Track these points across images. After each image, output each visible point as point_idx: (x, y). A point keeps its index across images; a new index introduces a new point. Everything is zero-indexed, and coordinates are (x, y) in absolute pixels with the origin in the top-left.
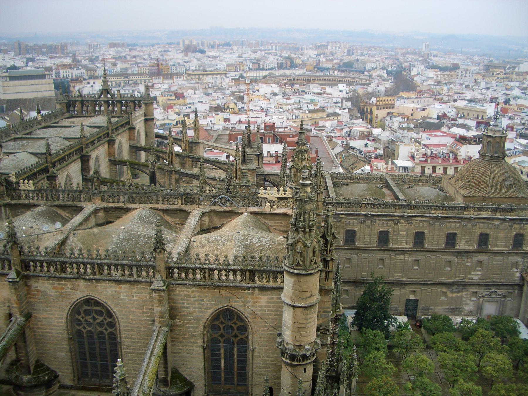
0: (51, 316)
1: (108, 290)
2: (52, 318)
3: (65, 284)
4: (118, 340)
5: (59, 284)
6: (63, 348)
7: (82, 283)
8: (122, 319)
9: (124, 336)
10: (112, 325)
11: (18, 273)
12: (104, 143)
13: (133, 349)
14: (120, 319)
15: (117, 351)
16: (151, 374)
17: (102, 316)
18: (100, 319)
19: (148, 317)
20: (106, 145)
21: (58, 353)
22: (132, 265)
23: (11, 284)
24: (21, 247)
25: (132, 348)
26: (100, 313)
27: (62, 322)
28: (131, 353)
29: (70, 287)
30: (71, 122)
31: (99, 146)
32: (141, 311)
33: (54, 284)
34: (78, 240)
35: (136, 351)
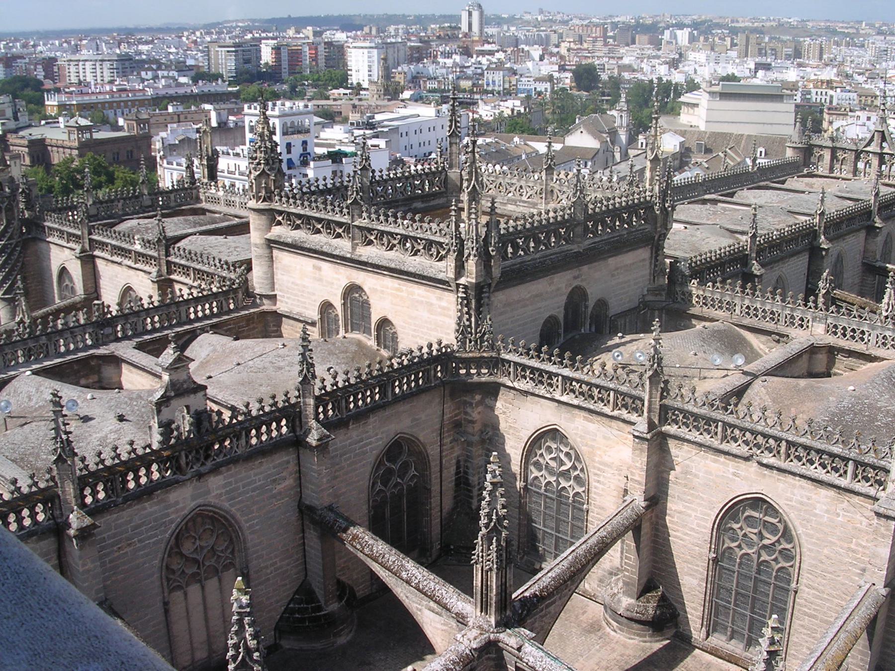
0: (689, 512)
1: (796, 491)
2: (690, 516)
3: (723, 463)
4: (793, 585)
5: (715, 461)
6: (697, 571)
7: (753, 469)
8: (810, 550)
9: (805, 581)
10: (787, 555)
11: (651, 426)
12: (858, 230)
13: (815, 610)
14: (803, 550)
15: (785, 605)
16: (830, 662)
17: (775, 535)
18: (769, 539)
19: (856, 559)
20: (862, 235)
21: (686, 577)
22: (849, 459)
23: (637, 440)
24: (666, 382)
25: (813, 606)
26: (773, 530)
27: (705, 528)
28: (810, 616)
29: (732, 470)
30: (807, 184)
31: (848, 234)
32: (846, 545)
33: (707, 458)
34: (767, 393)
35: (820, 616)
